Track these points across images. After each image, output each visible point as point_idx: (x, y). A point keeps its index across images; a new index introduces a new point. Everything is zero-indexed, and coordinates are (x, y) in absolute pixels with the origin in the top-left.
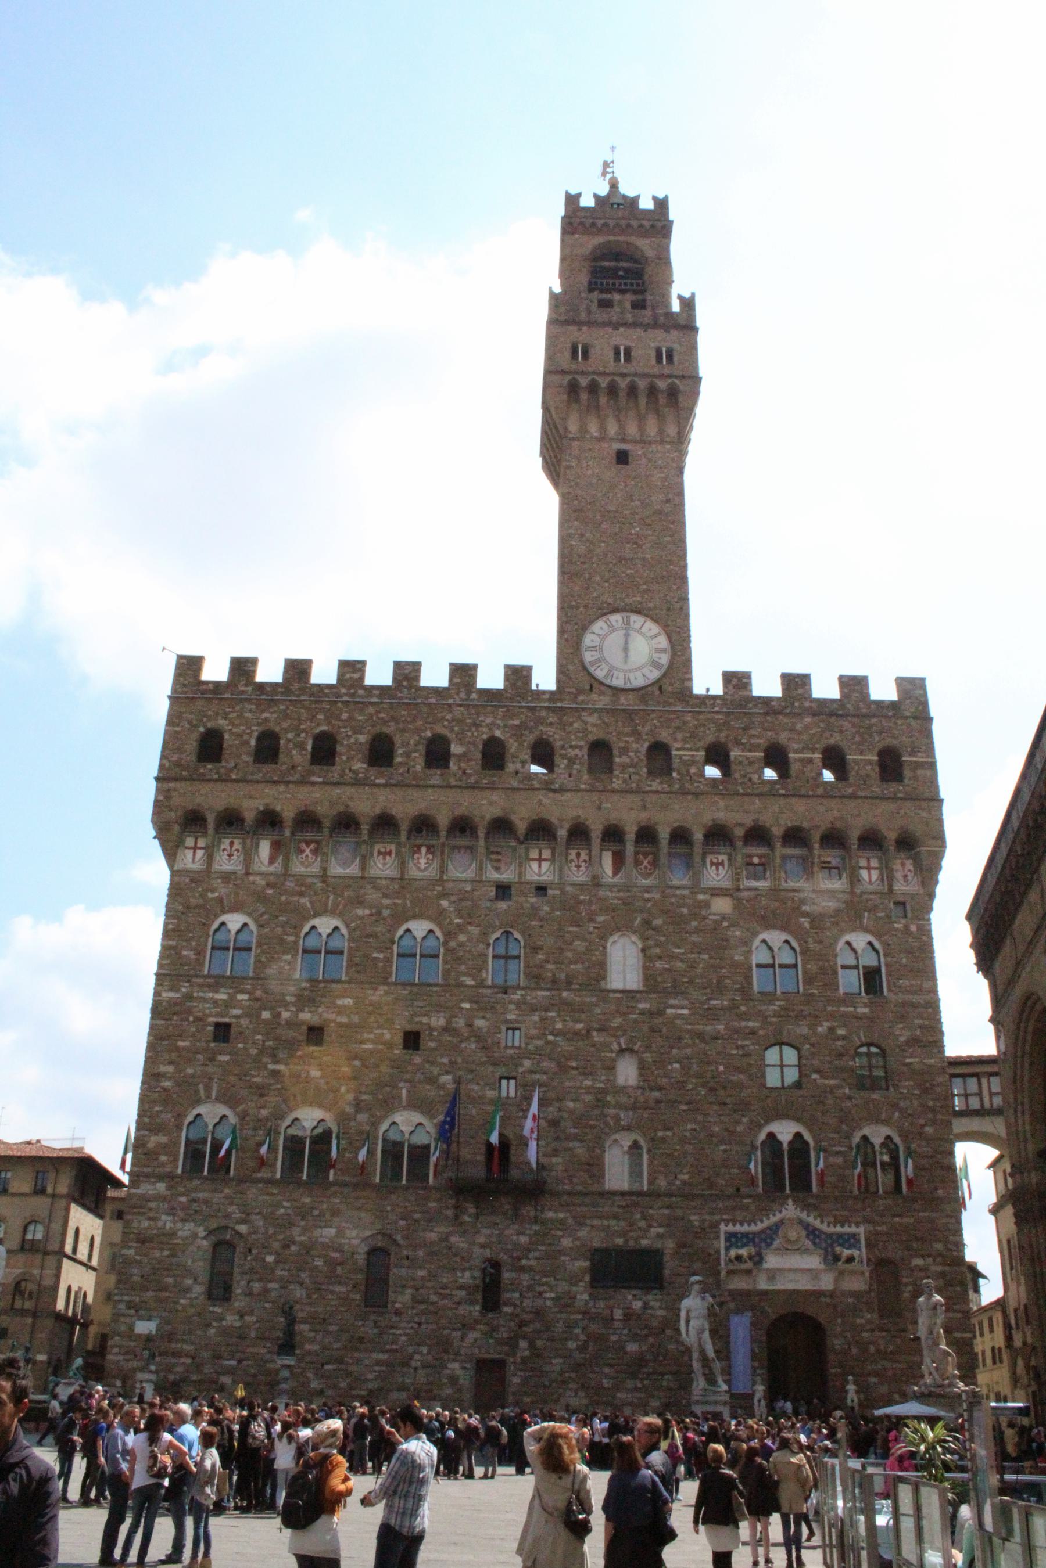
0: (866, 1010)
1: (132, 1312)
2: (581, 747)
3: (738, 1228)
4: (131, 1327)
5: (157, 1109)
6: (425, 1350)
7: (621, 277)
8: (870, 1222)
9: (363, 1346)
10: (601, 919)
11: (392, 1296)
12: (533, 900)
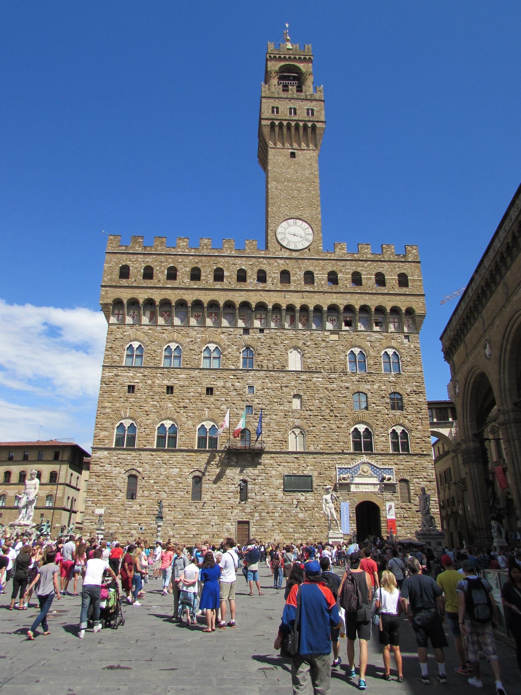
0: (394, 379)
1: (94, 505)
2: (277, 273)
3: (343, 466)
4: (93, 512)
6: (216, 518)
7: (291, 80)
8: (396, 464)
9: (190, 517)
10: (285, 342)
12: (259, 334)
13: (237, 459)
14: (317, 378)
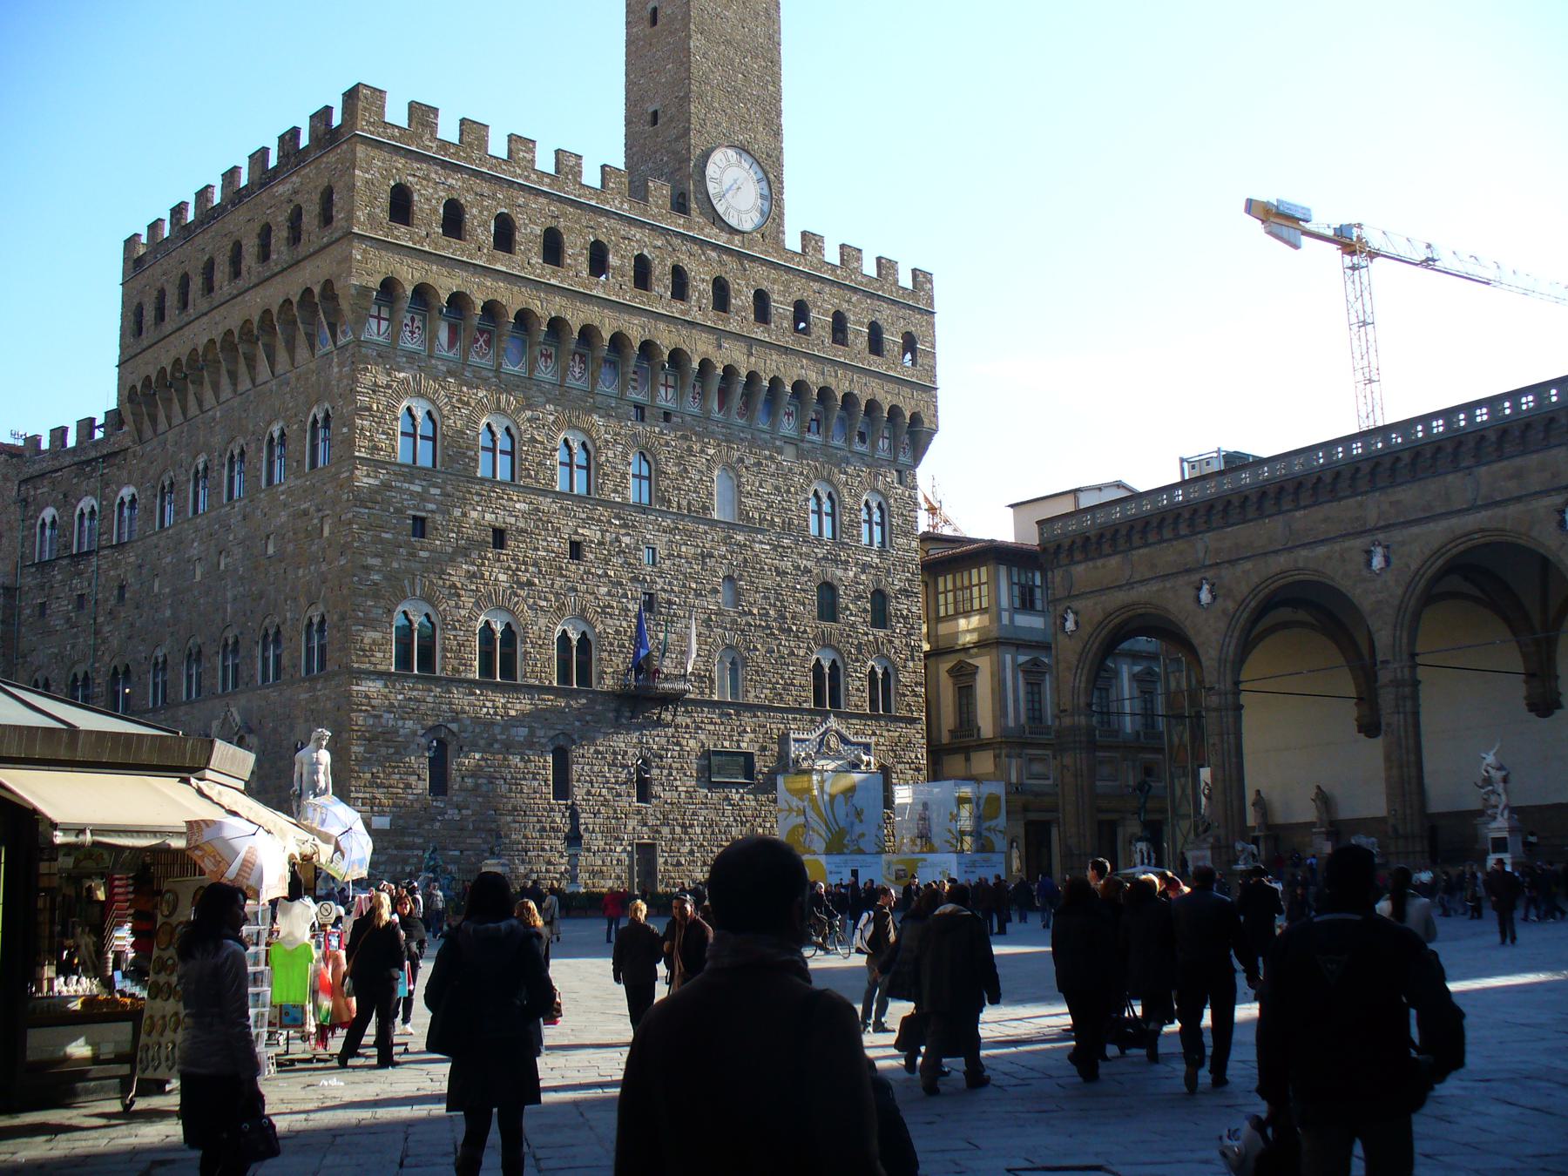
14: (761, 542)
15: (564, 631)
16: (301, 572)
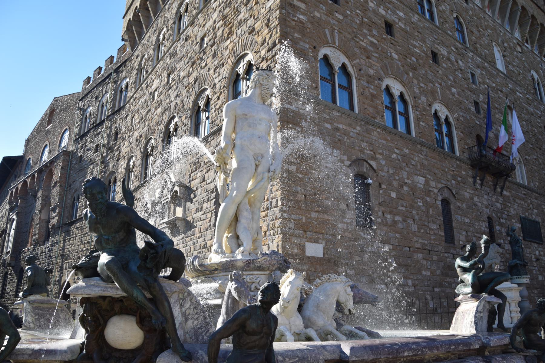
5: (296, 35)
11: (457, 236)
13: (482, 180)
15: (436, 111)
16: (229, 41)
